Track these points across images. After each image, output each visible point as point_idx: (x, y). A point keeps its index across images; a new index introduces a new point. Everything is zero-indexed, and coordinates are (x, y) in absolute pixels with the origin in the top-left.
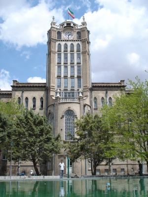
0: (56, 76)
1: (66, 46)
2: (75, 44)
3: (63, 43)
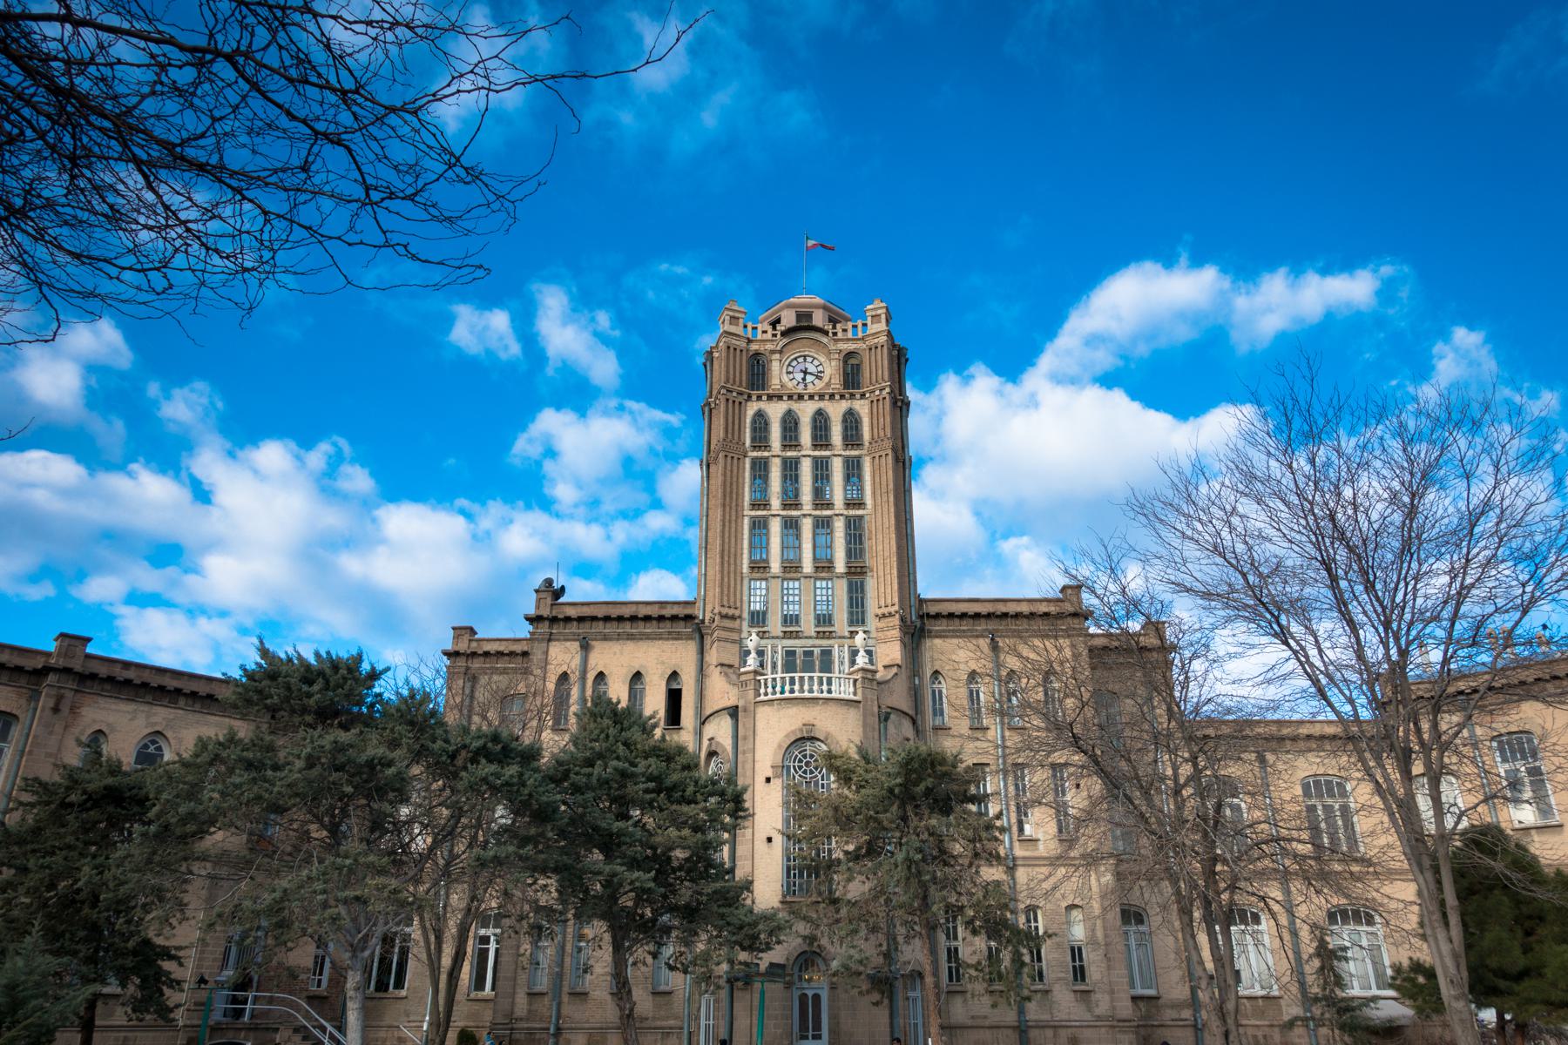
0: (745, 569)
1: (790, 425)
2: (836, 411)
3: (775, 411)
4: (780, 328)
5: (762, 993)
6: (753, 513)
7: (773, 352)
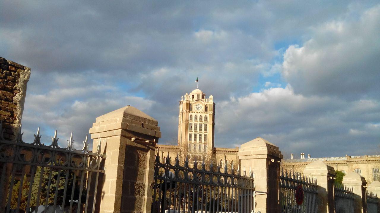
2: (203, 116)
7: (194, 104)
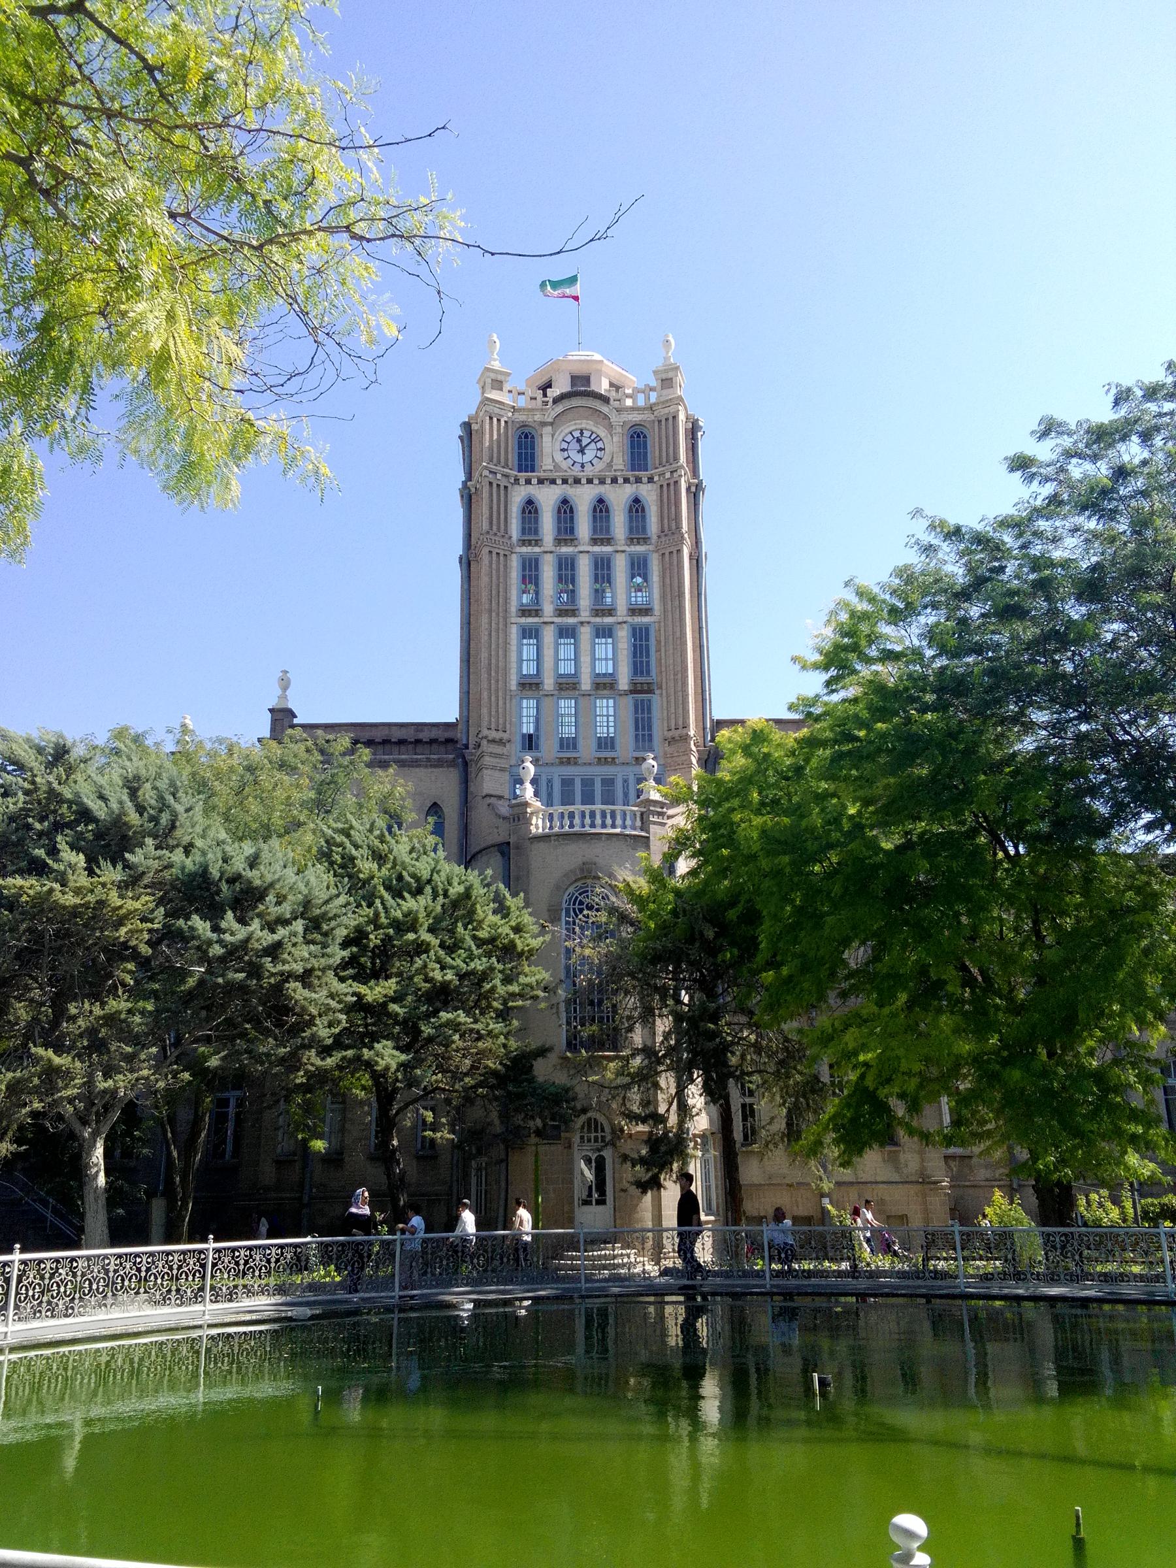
2: (619, 497)
4: (554, 392)
5: (537, 1155)
6: (523, 620)
